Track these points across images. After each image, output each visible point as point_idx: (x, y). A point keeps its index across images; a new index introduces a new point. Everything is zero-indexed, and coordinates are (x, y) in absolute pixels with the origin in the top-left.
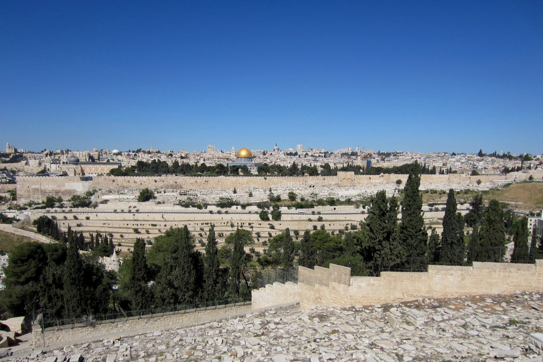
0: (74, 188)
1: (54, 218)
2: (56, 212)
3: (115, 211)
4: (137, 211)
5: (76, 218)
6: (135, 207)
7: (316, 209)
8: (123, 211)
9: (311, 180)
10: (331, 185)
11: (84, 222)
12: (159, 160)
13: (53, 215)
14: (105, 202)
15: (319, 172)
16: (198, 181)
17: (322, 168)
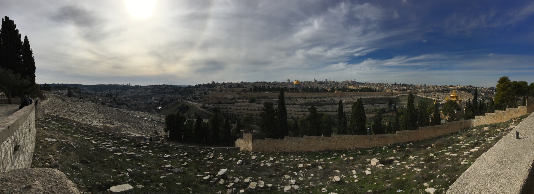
0: (227, 97)
1: (219, 107)
2: (220, 105)
3: (241, 106)
4: (249, 106)
5: (226, 108)
6: (248, 105)
7: (324, 107)
8: (243, 106)
9: (324, 94)
10: (332, 96)
11: (229, 110)
12: (262, 86)
13: (219, 106)
14: (237, 102)
15: (328, 91)
16: (275, 94)
17: (330, 89)
